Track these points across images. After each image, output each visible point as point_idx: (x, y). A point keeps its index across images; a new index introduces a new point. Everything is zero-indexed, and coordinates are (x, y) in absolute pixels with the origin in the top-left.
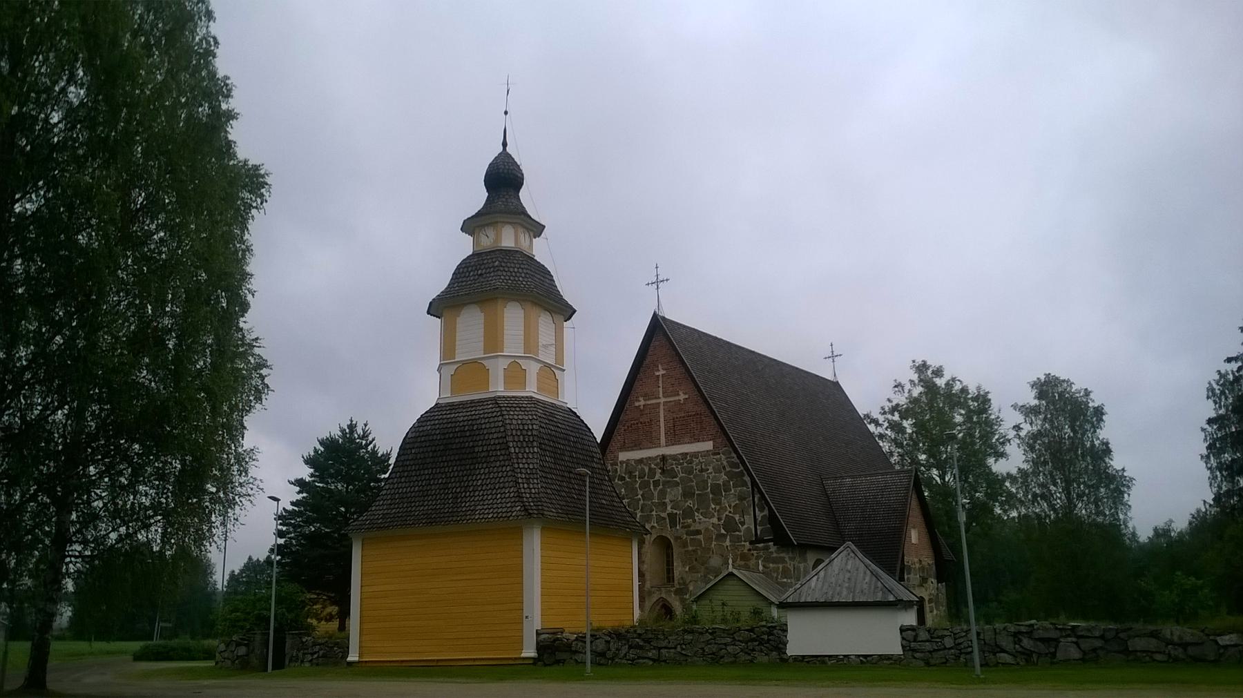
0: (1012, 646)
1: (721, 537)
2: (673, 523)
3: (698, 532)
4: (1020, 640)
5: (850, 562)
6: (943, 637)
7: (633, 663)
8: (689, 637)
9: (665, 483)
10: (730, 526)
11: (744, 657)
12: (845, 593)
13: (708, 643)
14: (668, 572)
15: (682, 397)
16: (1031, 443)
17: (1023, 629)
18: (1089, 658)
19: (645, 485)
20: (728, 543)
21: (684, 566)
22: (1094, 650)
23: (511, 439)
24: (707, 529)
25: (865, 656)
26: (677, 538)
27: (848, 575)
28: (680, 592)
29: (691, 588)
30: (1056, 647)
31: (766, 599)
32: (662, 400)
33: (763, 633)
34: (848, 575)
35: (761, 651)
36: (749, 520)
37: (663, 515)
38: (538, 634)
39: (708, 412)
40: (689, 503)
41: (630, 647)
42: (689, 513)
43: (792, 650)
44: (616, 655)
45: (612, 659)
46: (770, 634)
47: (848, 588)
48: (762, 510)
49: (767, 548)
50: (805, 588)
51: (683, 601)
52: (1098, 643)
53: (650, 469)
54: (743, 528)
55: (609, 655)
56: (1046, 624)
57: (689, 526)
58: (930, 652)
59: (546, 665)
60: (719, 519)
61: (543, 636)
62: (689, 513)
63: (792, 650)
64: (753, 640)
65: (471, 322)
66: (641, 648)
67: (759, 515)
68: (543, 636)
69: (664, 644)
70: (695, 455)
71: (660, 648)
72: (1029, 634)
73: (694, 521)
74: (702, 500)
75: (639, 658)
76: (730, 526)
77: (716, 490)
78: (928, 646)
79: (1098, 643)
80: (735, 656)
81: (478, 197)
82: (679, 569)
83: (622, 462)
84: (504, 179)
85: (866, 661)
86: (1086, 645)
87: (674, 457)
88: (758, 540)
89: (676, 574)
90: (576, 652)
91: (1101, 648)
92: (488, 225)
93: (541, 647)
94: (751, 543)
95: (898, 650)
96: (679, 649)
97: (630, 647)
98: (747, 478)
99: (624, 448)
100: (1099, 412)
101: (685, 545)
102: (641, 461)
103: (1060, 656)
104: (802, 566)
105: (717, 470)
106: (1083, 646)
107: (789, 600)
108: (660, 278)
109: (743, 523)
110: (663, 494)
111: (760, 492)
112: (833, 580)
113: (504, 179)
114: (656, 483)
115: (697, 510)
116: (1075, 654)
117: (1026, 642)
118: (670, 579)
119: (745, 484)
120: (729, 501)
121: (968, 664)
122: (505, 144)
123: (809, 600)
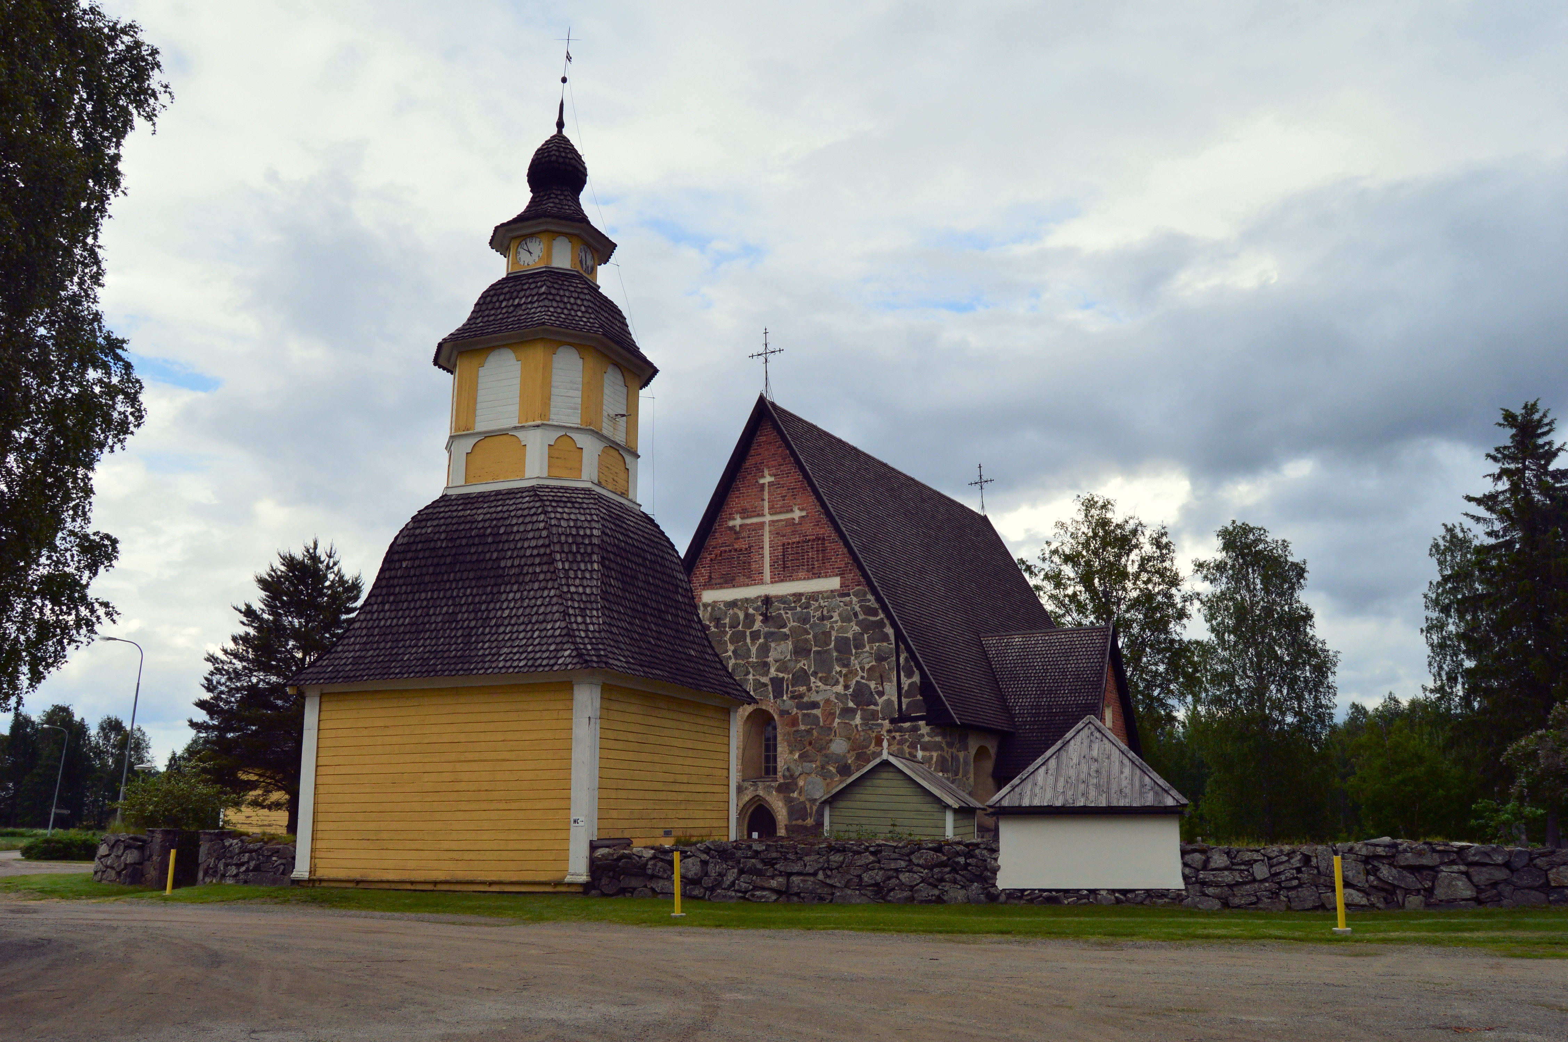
0: (1362, 877)
1: (847, 712)
2: (778, 694)
3: (815, 705)
4: (1376, 870)
5: (1095, 746)
6: (1250, 863)
7: (745, 897)
8: (837, 858)
9: (768, 635)
10: (862, 696)
11: (926, 891)
12: (1093, 793)
13: (867, 868)
14: (767, 758)
15: (797, 514)
16: (1212, 607)
17: (1380, 851)
18: (1485, 898)
19: (738, 637)
20: (858, 720)
21: (791, 752)
22: (1494, 885)
23: (558, 548)
24: (827, 701)
25: (1124, 892)
26: (783, 713)
27: (1094, 766)
28: (785, 789)
29: (801, 783)
30: (1434, 879)
31: (938, 801)
32: (768, 518)
33: (958, 854)
34: (1094, 766)
35: (955, 882)
36: (890, 689)
37: (764, 680)
38: (593, 847)
39: (834, 536)
40: (803, 664)
41: (741, 872)
42: (801, 677)
43: (1004, 881)
44: (718, 884)
45: (712, 889)
46: (969, 855)
47: (1097, 786)
48: (909, 675)
49: (916, 729)
50: (1029, 784)
51: (788, 801)
52: (1501, 874)
53: (747, 615)
54: (880, 701)
55: (707, 882)
56: (1419, 845)
57: (801, 696)
58: (1230, 886)
59: (604, 895)
60: (846, 687)
61: (600, 852)
62: (801, 677)
63: (1004, 881)
64: (942, 865)
65: (503, 378)
66: (759, 873)
67: (906, 683)
68: (600, 852)
69: (797, 868)
70: (814, 596)
71: (789, 875)
72: (1391, 859)
73: (809, 689)
74: (823, 662)
75: (755, 888)
76: (862, 696)
77: (843, 646)
78: (1227, 877)
79: (1501, 874)
80: (912, 888)
81: (517, 198)
82: (785, 757)
83: (706, 606)
84: (557, 171)
85: (1125, 900)
86: (1482, 876)
87: (782, 599)
88: (903, 717)
89: (781, 764)
90: (653, 877)
91: (1506, 882)
92: (532, 236)
93: (595, 866)
94: (893, 721)
95: (1177, 883)
96: (821, 876)
97: (741, 872)
98: (889, 631)
99: (710, 584)
100: (1300, 571)
101: (794, 722)
102: (733, 604)
103: (1440, 893)
104: (961, 755)
105: (846, 619)
106: (1475, 879)
107: (1005, 803)
108: (771, 348)
109: (881, 694)
110: (764, 650)
111: (908, 649)
112: (1072, 773)
113: (557, 171)
114: (755, 636)
115: (815, 674)
116: (1463, 889)
117: (1385, 872)
118: (770, 769)
119: (886, 638)
120: (863, 660)
121: (1325, 909)
122: (560, 124)
123: (1036, 802)
